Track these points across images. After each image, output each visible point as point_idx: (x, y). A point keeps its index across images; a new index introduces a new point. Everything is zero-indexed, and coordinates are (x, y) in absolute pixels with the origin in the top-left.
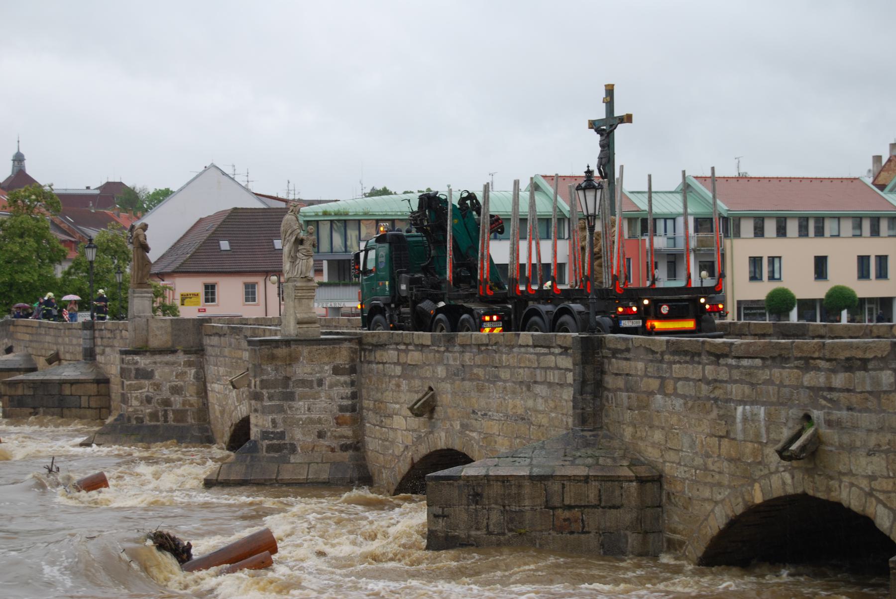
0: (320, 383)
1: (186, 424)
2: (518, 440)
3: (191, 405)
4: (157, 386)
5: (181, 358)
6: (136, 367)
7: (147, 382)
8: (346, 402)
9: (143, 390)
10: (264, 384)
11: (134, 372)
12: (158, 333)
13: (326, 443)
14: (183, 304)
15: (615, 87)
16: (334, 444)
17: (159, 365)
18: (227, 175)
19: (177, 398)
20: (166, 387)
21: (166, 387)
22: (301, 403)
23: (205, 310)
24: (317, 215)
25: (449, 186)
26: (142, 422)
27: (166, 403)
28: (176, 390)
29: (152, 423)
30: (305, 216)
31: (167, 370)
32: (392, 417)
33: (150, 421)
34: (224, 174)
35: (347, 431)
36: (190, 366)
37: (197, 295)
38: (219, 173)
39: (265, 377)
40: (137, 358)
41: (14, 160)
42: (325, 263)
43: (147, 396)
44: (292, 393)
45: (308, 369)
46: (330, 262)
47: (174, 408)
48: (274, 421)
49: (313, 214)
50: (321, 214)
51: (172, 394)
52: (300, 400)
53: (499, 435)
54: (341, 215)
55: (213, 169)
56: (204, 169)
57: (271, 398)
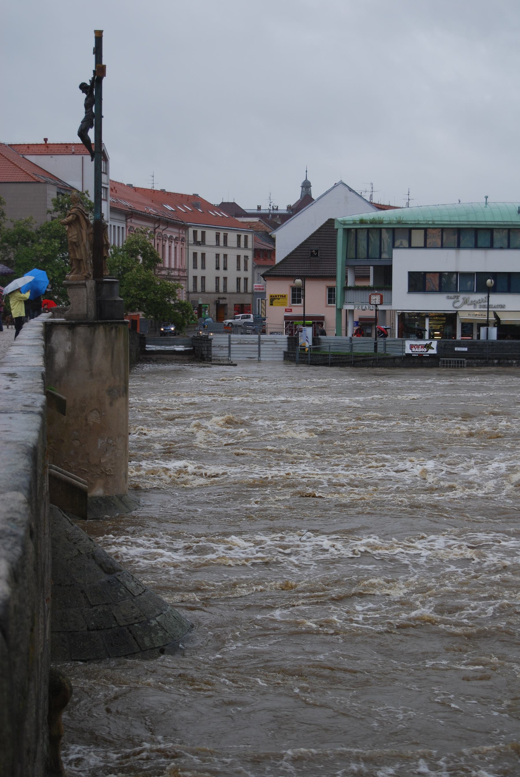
14: (271, 304)
15: (104, 34)
18: (354, 191)
23: (291, 310)
24: (354, 223)
25: (486, 197)
30: (345, 224)
34: (351, 190)
37: (285, 296)
38: (347, 189)
41: (302, 187)
42: (372, 268)
46: (375, 267)
49: (352, 222)
50: (358, 222)
54: (376, 223)
55: (341, 186)
56: (333, 185)
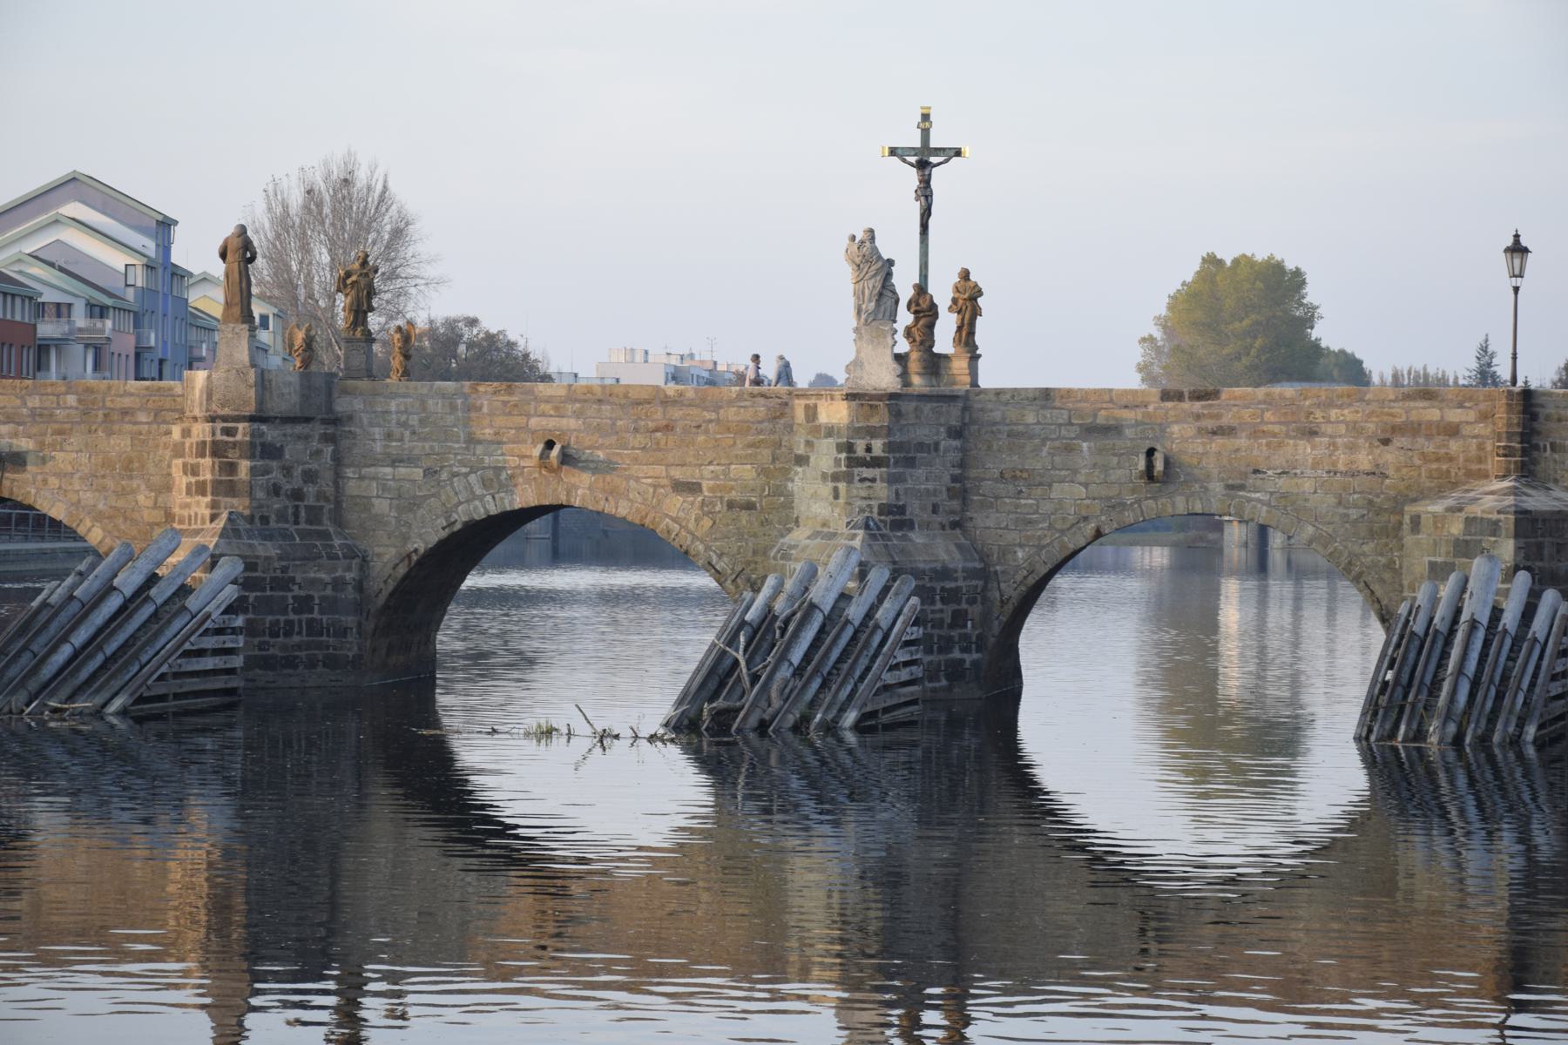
0: (937, 445)
1: (321, 528)
2: (1356, 496)
3: (327, 500)
4: (287, 471)
5: (318, 429)
6: (262, 440)
7: (274, 464)
8: (957, 471)
9: (270, 476)
10: (890, 447)
11: (259, 449)
12: (286, 391)
13: (939, 519)
16: (945, 521)
17: (289, 439)
19: (310, 489)
20: (298, 471)
21: (298, 471)
22: (920, 471)
26: (268, 523)
27: (297, 495)
28: (310, 477)
29: (280, 525)
31: (300, 446)
32: (1050, 486)
33: (278, 522)
35: (955, 504)
36: (326, 441)
39: (892, 439)
40: (264, 427)
43: (274, 485)
44: (913, 459)
45: (926, 431)
47: (306, 503)
48: (897, 494)
51: (305, 482)
52: (919, 468)
53: (1315, 492)
57: (896, 463)
